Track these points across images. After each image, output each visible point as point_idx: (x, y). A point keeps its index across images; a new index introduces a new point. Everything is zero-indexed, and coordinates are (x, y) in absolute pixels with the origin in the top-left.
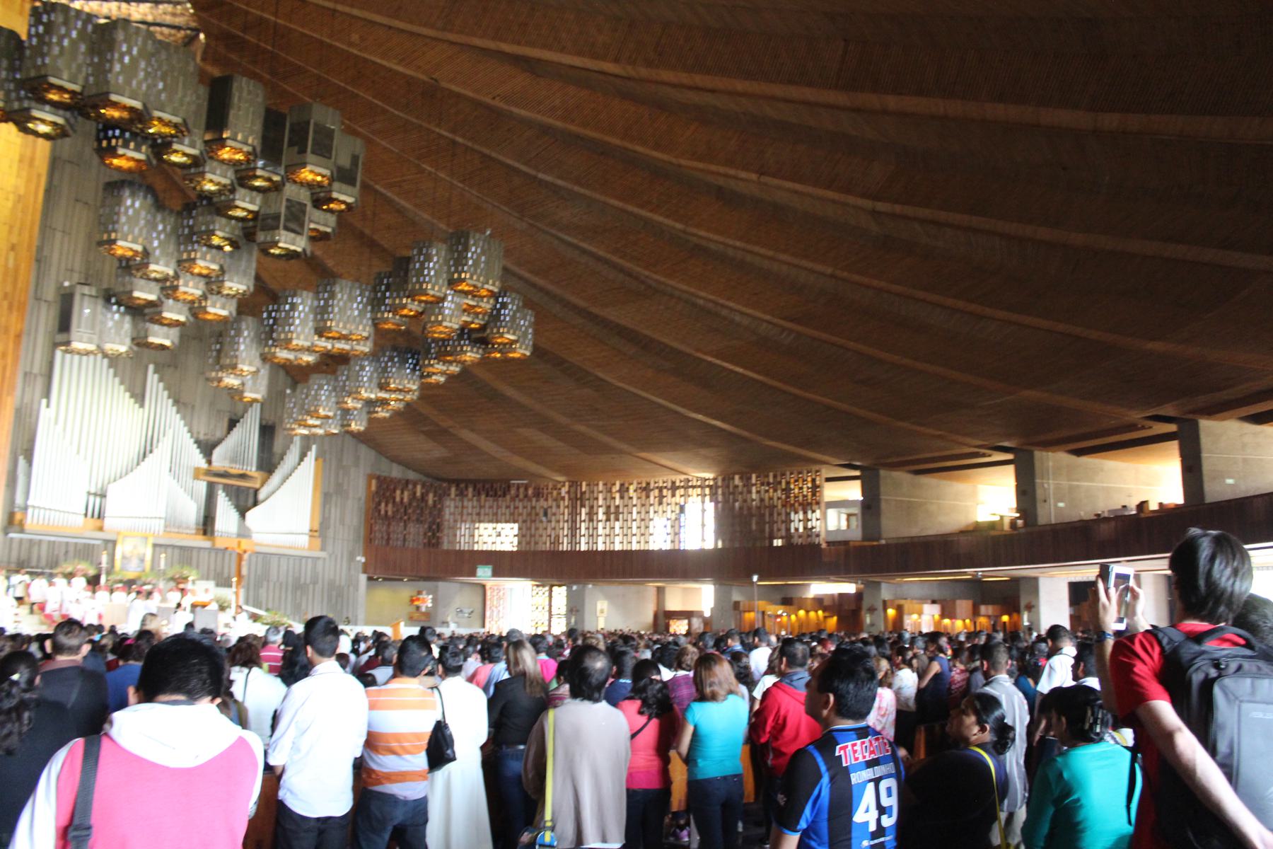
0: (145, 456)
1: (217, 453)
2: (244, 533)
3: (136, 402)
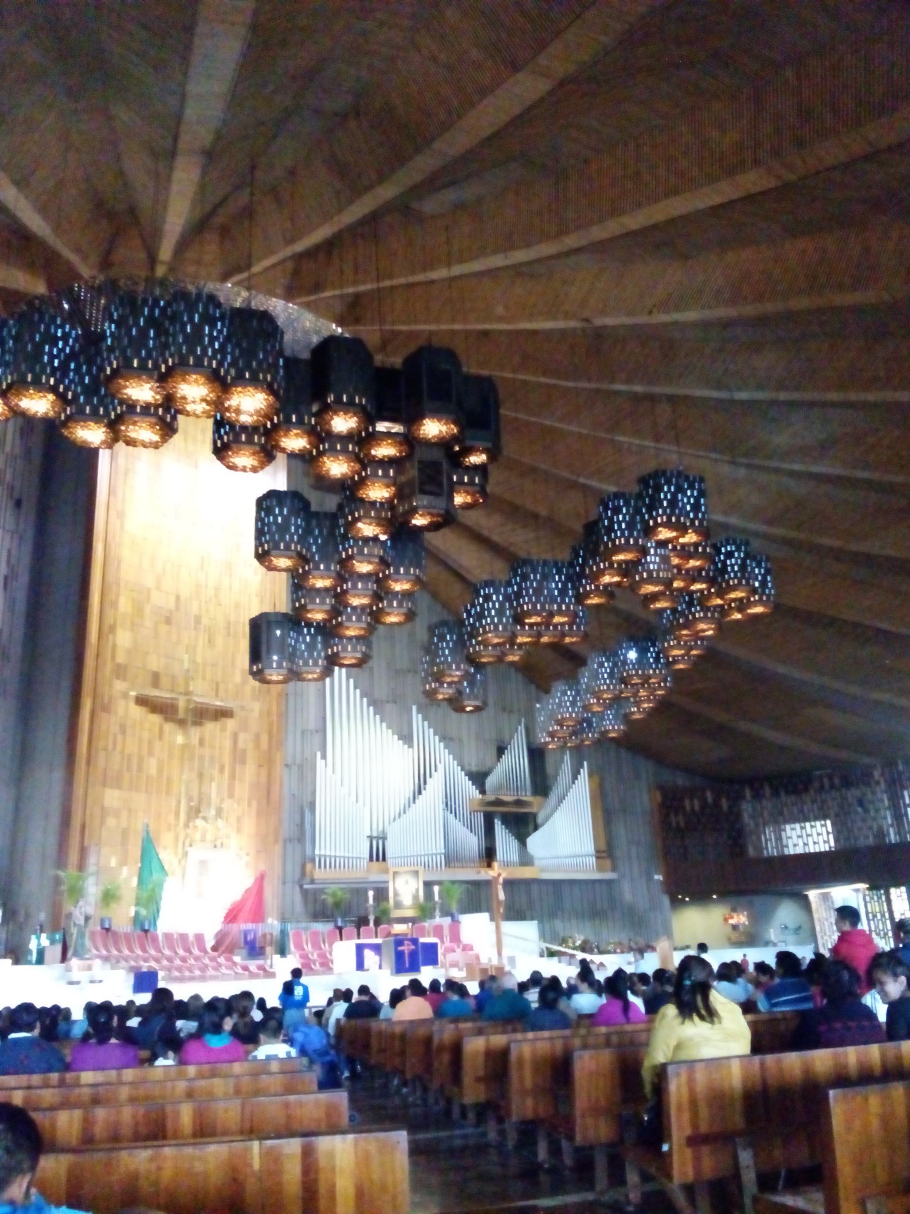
0: (420, 793)
1: (490, 782)
2: (526, 860)
3: (405, 743)
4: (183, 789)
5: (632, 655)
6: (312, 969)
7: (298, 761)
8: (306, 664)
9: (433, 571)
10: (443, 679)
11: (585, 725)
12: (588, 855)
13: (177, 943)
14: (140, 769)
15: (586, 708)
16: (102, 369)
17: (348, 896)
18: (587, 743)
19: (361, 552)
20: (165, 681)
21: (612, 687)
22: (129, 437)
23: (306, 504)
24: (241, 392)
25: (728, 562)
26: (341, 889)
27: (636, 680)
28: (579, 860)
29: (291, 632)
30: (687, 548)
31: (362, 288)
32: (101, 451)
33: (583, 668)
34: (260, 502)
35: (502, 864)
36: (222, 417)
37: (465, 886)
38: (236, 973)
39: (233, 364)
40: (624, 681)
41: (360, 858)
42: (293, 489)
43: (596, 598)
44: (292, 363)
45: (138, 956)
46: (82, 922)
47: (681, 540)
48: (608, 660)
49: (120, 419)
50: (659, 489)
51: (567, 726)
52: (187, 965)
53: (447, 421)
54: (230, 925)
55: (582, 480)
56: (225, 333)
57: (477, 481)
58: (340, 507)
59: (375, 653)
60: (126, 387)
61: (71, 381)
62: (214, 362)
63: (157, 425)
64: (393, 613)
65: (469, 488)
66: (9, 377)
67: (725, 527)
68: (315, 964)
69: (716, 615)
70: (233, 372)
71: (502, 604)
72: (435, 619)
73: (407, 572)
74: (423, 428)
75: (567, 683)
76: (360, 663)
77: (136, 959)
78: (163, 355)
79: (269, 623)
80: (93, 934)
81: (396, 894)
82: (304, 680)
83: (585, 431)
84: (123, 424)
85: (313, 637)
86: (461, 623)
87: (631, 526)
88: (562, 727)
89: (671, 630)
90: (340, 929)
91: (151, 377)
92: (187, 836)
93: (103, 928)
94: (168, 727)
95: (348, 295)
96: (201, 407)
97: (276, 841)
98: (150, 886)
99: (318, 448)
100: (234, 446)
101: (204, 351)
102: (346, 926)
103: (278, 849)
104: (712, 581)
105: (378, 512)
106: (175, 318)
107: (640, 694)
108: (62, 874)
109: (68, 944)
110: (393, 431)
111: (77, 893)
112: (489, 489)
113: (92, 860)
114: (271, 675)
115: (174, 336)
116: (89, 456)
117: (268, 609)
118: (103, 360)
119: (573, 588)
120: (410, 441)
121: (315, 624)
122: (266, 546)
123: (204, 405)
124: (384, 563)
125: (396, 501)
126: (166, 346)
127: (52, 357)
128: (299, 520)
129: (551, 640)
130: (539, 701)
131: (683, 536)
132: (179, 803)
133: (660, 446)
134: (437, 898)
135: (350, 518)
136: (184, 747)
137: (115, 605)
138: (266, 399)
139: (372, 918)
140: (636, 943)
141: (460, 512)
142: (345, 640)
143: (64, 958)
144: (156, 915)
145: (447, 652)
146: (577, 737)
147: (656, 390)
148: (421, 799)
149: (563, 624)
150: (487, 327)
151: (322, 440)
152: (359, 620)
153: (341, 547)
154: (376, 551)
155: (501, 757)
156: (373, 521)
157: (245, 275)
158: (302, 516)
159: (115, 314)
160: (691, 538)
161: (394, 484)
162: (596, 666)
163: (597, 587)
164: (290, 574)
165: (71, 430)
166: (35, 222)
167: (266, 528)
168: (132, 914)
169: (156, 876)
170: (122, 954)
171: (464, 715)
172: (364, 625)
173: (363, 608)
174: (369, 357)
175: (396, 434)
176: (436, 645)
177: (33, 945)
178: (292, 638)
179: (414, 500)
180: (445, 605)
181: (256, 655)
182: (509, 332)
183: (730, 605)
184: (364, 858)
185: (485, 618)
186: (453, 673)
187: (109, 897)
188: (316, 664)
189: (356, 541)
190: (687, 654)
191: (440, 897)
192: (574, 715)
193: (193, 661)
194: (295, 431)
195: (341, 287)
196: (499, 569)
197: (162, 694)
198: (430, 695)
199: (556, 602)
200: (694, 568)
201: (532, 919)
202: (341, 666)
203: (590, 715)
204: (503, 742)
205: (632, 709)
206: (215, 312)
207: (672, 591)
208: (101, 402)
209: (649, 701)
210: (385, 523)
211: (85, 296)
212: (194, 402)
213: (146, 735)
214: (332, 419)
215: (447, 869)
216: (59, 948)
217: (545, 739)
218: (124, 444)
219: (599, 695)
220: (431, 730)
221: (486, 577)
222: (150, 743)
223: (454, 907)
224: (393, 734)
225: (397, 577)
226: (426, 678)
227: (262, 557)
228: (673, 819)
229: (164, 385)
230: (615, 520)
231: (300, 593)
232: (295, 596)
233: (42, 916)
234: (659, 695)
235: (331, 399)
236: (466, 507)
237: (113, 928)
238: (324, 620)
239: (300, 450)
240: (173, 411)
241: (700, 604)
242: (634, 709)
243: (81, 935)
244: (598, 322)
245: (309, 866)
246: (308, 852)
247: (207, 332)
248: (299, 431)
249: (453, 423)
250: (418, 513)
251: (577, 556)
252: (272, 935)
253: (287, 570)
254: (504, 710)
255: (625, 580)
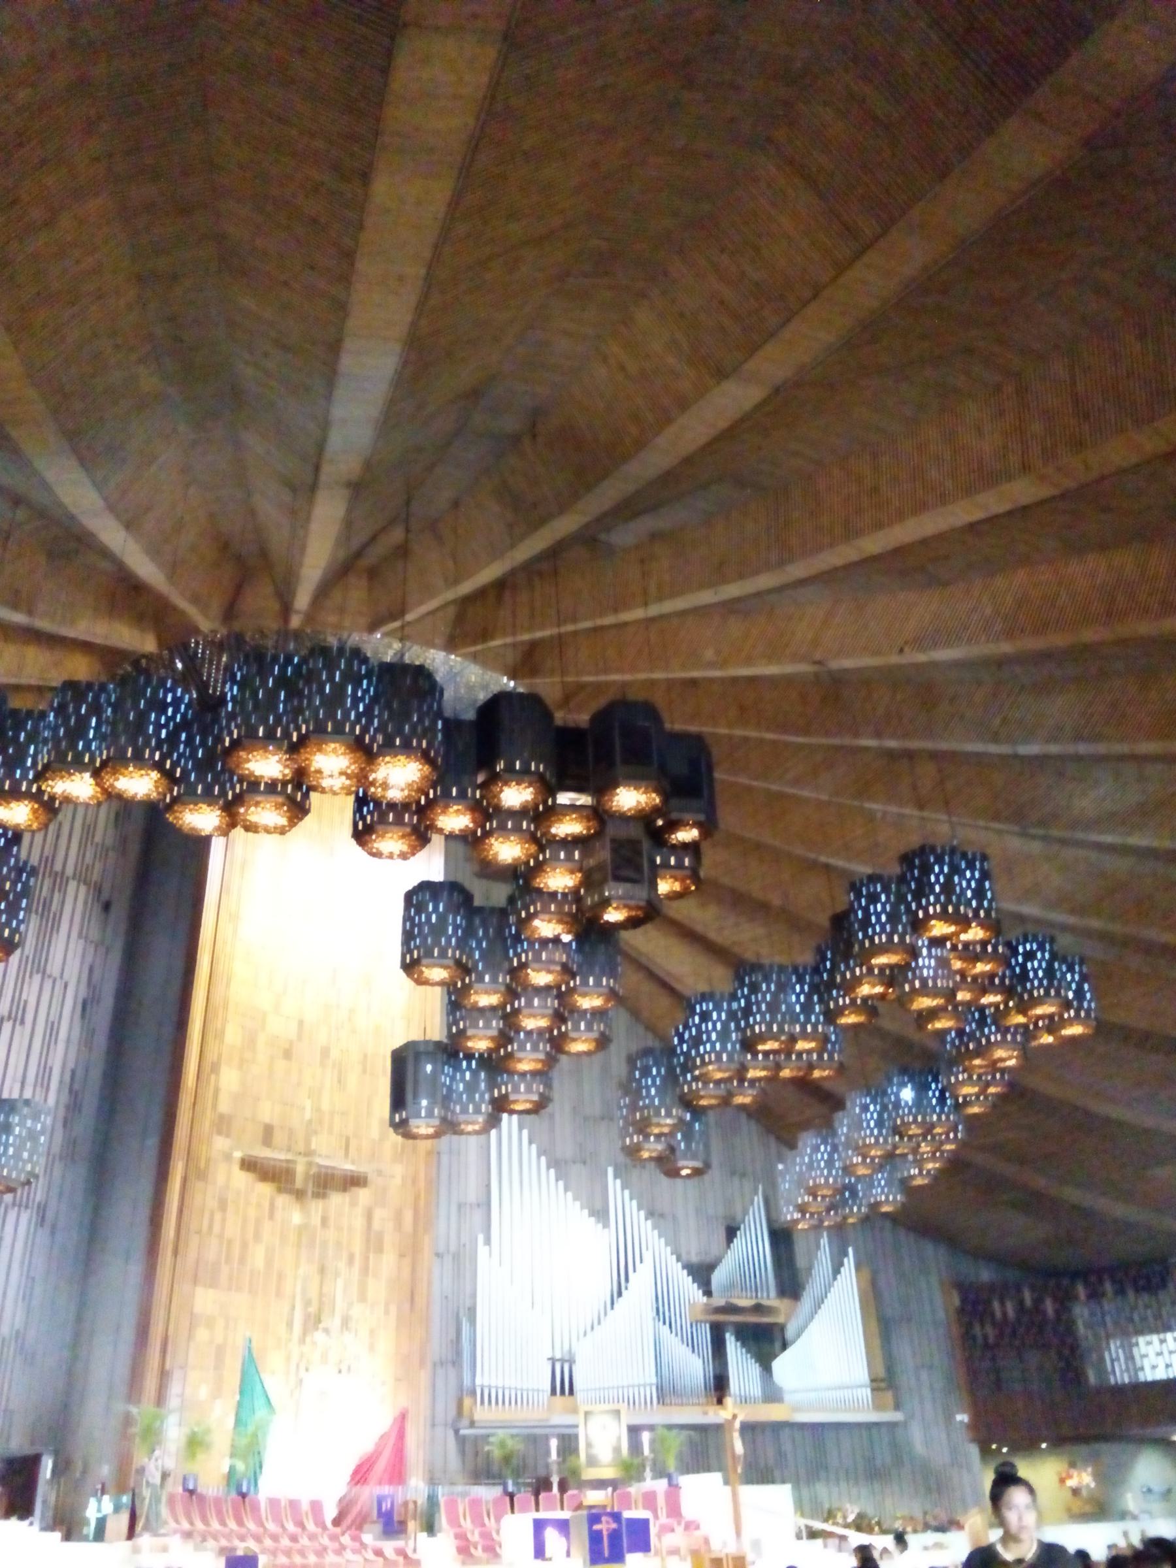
0: (620, 1294)
1: (719, 1277)
2: (772, 1394)
3: (598, 1221)
4: (298, 1289)
5: (907, 1094)
6: (471, 1555)
7: (453, 1248)
8: (464, 1111)
9: (631, 979)
10: (649, 1130)
11: (847, 1194)
12: (861, 1386)
13: (286, 1516)
14: (242, 1260)
15: (847, 1170)
16: (219, 739)
17: (520, 1447)
18: (851, 1220)
19: (537, 958)
20: (279, 1137)
21: (881, 1140)
22: (250, 821)
23: (468, 897)
24: (388, 762)
25: (1029, 965)
26: (513, 1436)
27: (914, 1130)
28: (847, 1394)
29: (446, 1067)
30: (971, 948)
31: (539, 634)
32: (214, 839)
33: (840, 1114)
34: (409, 896)
35: (738, 1399)
36: (365, 793)
37: (685, 1433)
38: (366, 1560)
39: (381, 729)
40: (897, 1131)
41: (538, 1390)
42: (452, 879)
43: (853, 1016)
44: (453, 726)
45: (232, 1531)
46: (157, 1480)
47: (964, 937)
48: (874, 1102)
49: (239, 799)
50: (926, 870)
51: (823, 1197)
52: (297, 1546)
53: (646, 789)
54: (358, 1486)
55: (823, 859)
56: (372, 693)
57: (687, 862)
58: (511, 900)
59: (556, 1095)
60: (248, 761)
61: (180, 756)
62: (358, 728)
63: (283, 805)
64: (580, 1038)
65: (678, 873)
66: (105, 752)
67: (1021, 919)
68: (476, 1548)
69: (1019, 1038)
70: (380, 738)
71: (725, 1025)
72: (634, 1047)
73: (598, 983)
74: (616, 798)
75: (819, 1134)
76: (538, 1108)
77: (228, 1537)
78: (295, 721)
79: (418, 1056)
80: (171, 1500)
81: (589, 1445)
82: (462, 1133)
83: (824, 797)
84: (243, 806)
85: (475, 1074)
86: (672, 1051)
87: (893, 918)
88: (815, 1197)
89: (960, 1058)
90: (511, 1496)
91: (279, 748)
92: (302, 1355)
93: (186, 1490)
94: (283, 1200)
95: (523, 643)
96: (339, 782)
97: (422, 1363)
98: (251, 1429)
99: (483, 827)
100: (380, 828)
101: (346, 715)
102: (519, 1491)
103: (424, 1377)
104: (1009, 992)
105: (560, 905)
106: (311, 677)
107: (921, 1150)
108: (134, 1410)
109: (138, 1512)
110: (578, 803)
111: (152, 1436)
112: (702, 874)
113: (174, 1389)
114: (418, 1127)
115: (310, 699)
116: (199, 846)
117: (415, 1035)
118: (221, 729)
119: (820, 1001)
120: (599, 815)
121: (477, 1055)
122: (416, 953)
123: (343, 778)
124: (567, 971)
125: (582, 891)
126: (299, 711)
127: (158, 727)
128: (459, 918)
129: (795, 1074)
130: (781, 1159)
131: (965, 931)
132: (293, 1308)
133: (926, 814)
134: (646, 1451)
135: (523, 914)
136: (302, 1229)
137: (221, 1035)
138: (421, 770)
139: (555, 1480)
140: (935, 1518)
141: (666, 902)
142: (516, 1077)
143: (131, 1534)
144: (258, 1470)
145: (653, 1091)
146: (836, 1213)
147: (915, 744)
148: (620, 1303)
149: (809, 1052)
150: (695, 674)
151: (488, 817)
152: (535, 1048)
153: (511, 952)
154: (557, 956)
155: (732, 1242)
156: (552, 916)
157: (397, 624)
158: (462, 911)
159: (239, 675)
160: (975, 933)
161: (580, 870)
162: (857, 1110)
163: (853, 1001)
164: (445, 989)
165: (178, 814)
166: (146, 569)
167: (416, 930)
168: (226, 1470)
169: (261, 1413)
170: (211, 1529)
171: (679, 1181)
172: (542, 1056)
173: (541, 1032)
174: (548, 715)
175: (582, 806)
176: (639, 1081)
177: (92, 1512)
178: (447, 1075)
179: (606, 888)
180: (650, 1028)
181: (398, 1100)
182: (722, 680)
183: (1036, 1024)
184: (543, 1391)
185: (704, 1044)
186: (662, 1122)
187: (195, 1444)
188: (477, 1111)
189: (531, 943)
190: (983, 1091)
191: (652, 1450)
192: (831, 1180)
193: (318, 1110)
194: (455, 807)
195: (514, 634)
196: (720, 977)
197: (274, 1155)
198: (632, 1152)
199: (798, 1021)
200: (983, 974)
201: (783, 1482)
202: (512, 1112)
203: (853, 1180)
204: (734, 1219)
205: (912, 1172)
206: (360, 669)
207: (955, 1007)
208: (216, 780)
209: (933, 1158)
210: (569, 919)
211: (203, 653)
212: (331, 776)
213: (252, 1213)
214: (502, 791)
215: (661, 1406)
216: (125, 1518)
217: (792, 1216)
218: (242, 830)
219: (864, 1150)
220: (634, 1203)
221: (703, 987)
222: (258, 1222)
223: (671, 1464)
224: (582, 1208)
225: (586, 989)
226: (625, 1128)
227: (410, 967)
228: (977, 1330)
229: (295, 756)
230: (872, 911)
231: (458, 1014)
232: (451, 1017)
233: (105, 1471)
234: (948, 1151)
235: (500, 766)
236: (674, 896)
237: (199, 1490)
238: (490, 1051)
239: (460, 830)
240: (304, 787)
241: (995, 1022)
242: (914, 1171)
243: (156, 1499)
244: (836, 664)
245: (467, 1402)
246: (467, 1381)
247: (349, 692)
248: (460, 807)
249: (654, 792)
250: (610, 905)
251: (824, 959)
252: (415, 1503)
253: (442, 983)
254: (733, 1173)
255: (891, 990)
